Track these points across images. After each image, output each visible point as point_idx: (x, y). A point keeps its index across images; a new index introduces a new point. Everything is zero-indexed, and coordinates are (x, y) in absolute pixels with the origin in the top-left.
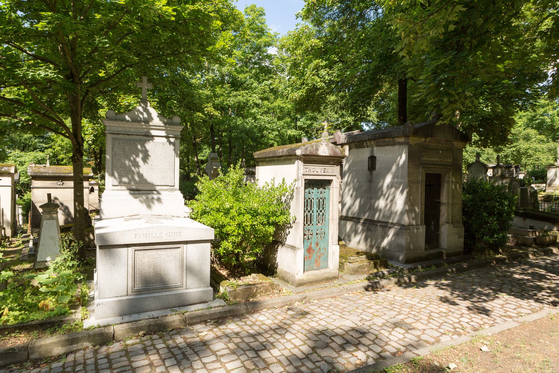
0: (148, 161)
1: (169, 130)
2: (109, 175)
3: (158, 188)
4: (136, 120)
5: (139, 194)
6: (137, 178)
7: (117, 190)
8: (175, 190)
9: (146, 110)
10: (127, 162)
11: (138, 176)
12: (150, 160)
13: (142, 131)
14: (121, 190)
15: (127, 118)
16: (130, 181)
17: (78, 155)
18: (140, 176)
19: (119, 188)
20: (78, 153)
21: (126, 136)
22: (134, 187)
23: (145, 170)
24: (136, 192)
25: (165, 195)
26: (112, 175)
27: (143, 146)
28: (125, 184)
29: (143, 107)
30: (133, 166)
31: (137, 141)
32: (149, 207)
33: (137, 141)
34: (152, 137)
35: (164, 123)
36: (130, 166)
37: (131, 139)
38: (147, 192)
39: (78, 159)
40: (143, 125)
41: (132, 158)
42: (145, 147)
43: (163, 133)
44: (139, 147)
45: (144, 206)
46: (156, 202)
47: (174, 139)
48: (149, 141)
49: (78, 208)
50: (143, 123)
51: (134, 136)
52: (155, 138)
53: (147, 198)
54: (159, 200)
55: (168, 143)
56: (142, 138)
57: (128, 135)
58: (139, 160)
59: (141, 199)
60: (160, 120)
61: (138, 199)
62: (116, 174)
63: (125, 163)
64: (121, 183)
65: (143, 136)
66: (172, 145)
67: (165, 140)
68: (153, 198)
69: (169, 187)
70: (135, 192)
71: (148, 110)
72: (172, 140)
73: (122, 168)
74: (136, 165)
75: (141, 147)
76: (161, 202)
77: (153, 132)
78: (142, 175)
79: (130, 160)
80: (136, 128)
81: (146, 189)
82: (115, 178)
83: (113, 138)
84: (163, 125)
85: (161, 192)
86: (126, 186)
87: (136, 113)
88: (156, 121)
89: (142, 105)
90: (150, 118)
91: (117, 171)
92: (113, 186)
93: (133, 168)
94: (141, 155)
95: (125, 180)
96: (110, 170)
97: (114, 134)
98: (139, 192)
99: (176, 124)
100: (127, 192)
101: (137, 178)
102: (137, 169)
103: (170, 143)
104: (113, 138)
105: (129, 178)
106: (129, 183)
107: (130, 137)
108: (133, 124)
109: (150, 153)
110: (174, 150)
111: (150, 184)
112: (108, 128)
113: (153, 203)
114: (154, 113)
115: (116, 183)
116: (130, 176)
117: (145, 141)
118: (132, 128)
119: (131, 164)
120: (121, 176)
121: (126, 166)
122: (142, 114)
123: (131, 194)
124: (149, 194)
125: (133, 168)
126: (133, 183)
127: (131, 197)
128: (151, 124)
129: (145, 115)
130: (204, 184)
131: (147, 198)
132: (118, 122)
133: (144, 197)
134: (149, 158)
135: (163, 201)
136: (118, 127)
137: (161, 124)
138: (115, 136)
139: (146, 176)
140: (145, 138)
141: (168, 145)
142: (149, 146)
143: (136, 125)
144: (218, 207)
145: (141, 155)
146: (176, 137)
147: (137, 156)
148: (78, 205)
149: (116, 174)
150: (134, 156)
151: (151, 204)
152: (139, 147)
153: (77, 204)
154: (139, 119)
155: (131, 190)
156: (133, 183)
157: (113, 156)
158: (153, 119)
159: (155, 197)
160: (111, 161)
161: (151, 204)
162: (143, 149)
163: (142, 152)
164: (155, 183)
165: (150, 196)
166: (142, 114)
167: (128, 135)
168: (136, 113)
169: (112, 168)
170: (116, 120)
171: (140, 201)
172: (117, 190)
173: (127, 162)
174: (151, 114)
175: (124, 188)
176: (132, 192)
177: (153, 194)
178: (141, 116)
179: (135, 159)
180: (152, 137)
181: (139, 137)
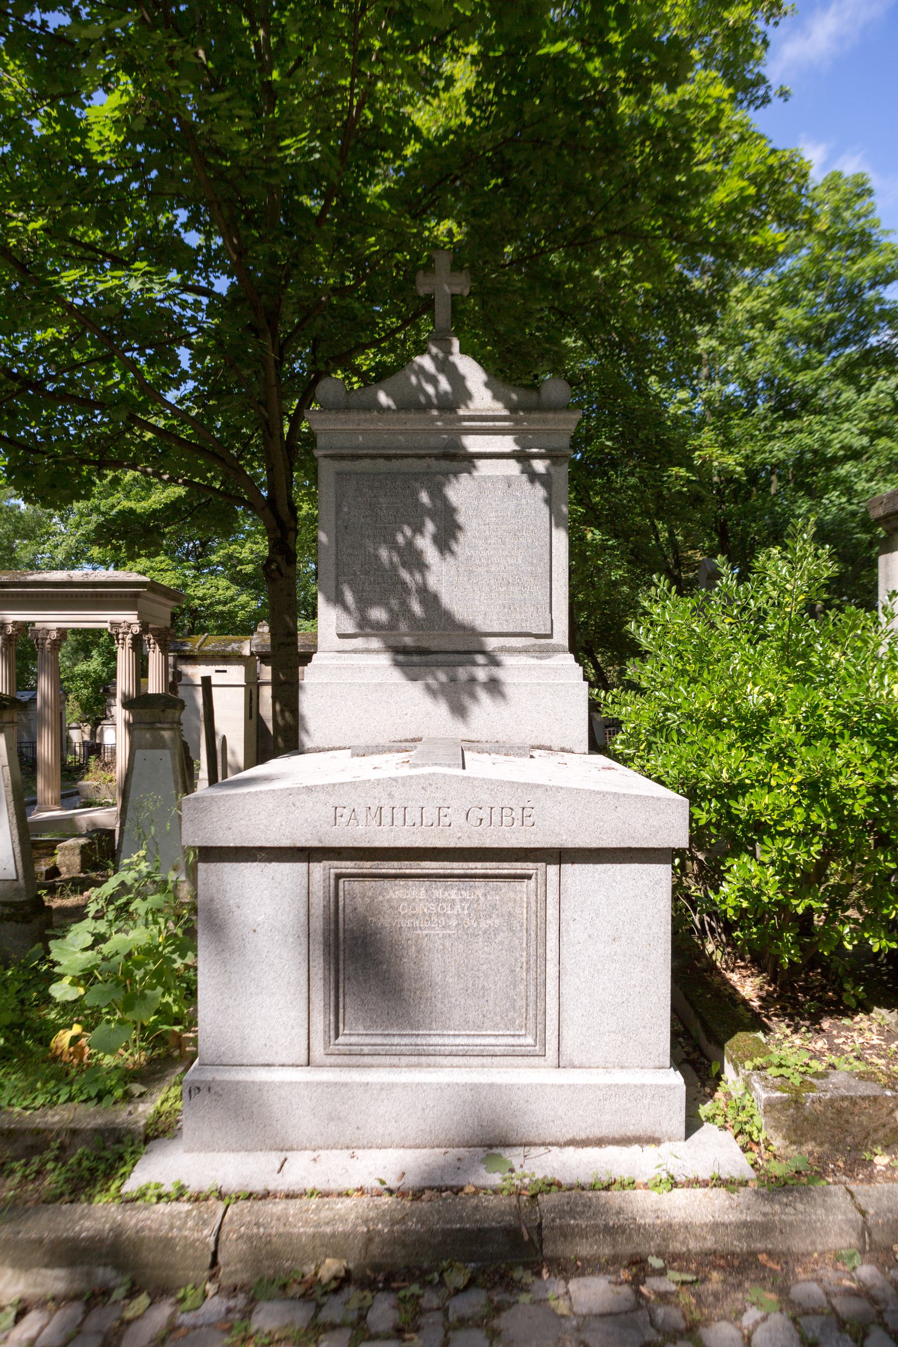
0: (455, 547)
2: (328, 600)
3: (492, 644)
4: (411, 404)
5: (427, 665)
6: (417, 608)
8: (556, 650)
10: (384, 553)
11: (422, 602)
12: (463, 546)
13: (432, 440)
14: (367, 651)
15: (383, 398)
17: (279, 558)
18: (430, 599)
19: (359, 643)
21: (381, 461)
22: (408, 641)
23: (443, 576)
24: (416, 659)
25: (516, 670)
26: (337, 600)
27: (438, 494)
29: (434, 358)
30: (404, 564)
32: (459, 711)
34: (468, 460)
35: (513, 408)
36: (394, 568)
38: (452, 658)
39: (279, 569)
41: (400, 539)
42: (445, 500)
43: (507, 444)
46: (483, 696)
47: (547, 462)
48: (456, 474)
49: (280, 721)
50: (435, 413)
52: (480, 463)
53: (453, 680)
54: (494, 686)
55: (524, 477)
57: (388, 457)
58: (425, 544)
59: (431, 681)
60: (496, 397)
61: (419, 684)
62: (349, 597)
63: (377, 557)
64: (366, 627)
65: (437, 457)
66: (538, 485)
67: (513, 468)
68: (473, 680)
69: (531, 641)
70: (412, 658)
71: (454, 366)
72: (540, 466)
73: (367, 573)
74: (416, 562)
75: (432, 496)
76: (502, 695)
77: (473, 444)
78: (435, 598)
79: (393, 546)
80: (415, 432)
81: (451, 647)
82: (346, 608)
83: (338, 473)
84: (505, 413)
85: (508, 660)
86: (384, 638)
90: (462, 393)
92: (342, 636)
93: (405, 575)
94: (430, 527)
95: (378, 614)
96: (332, 583)
99: (555, 408)
100: (384, 660)
101: (417, 608)
102: (418, 577)
103: (533, 477)
104: (338, 473)
105: (390, 611)
106: (392, 626)
107: (396, 464)
108: (403, 416)
109: (461, 519)
110: (548, 501)
112: (321, 441)
113: (473, 696)
115: (349, 627)
116: (394, 603)
118: (401, 432)
119: (396, 559)
120: (364, 604)
122: (434, 381)
123: (397, 664)
124: (461, 664)
125: (405, 575)
126: (403, 627)
127: (396, 676)
128: (461, 412)
129: (444, 385)
130: (663, 616)
131: (453, 680)
132: (354, 416)
133: (442, 677)
134: (461, 537)
135: (508, 690)
137: (499, 409)
138: (346, 465)
139: (448, 600)
140: (444, 464)
141: (527, 486)
142: (460, 492)
143: (413, 422)
144: (714, 706)
145: (430, 527)
146: (551, 456)
147: (419, 529)
148: (282, 711)
149: (349, 597)
150: (408, 532)
151: (467, 701)
152: (424, 497)
153: (278, 707)
154: (423, 399)
156: (403, 627)
157: (341, 532)
159: (481, 674)
160: (333, 551)
161: (467, 701)
162: (439, 504)
164: (482, 625)
165: (462, 673)
166: (434, 381)
167: (388, 457)
168: (414, 380)
169: (337, 576)
171: (429, 689)
172: (355, 651)
174: (462, 378)
175: (375, 643)
176: (401, 658)
177: (475, 664)
178: (430, 389)
179: (410, 543)
180: (468, 460)
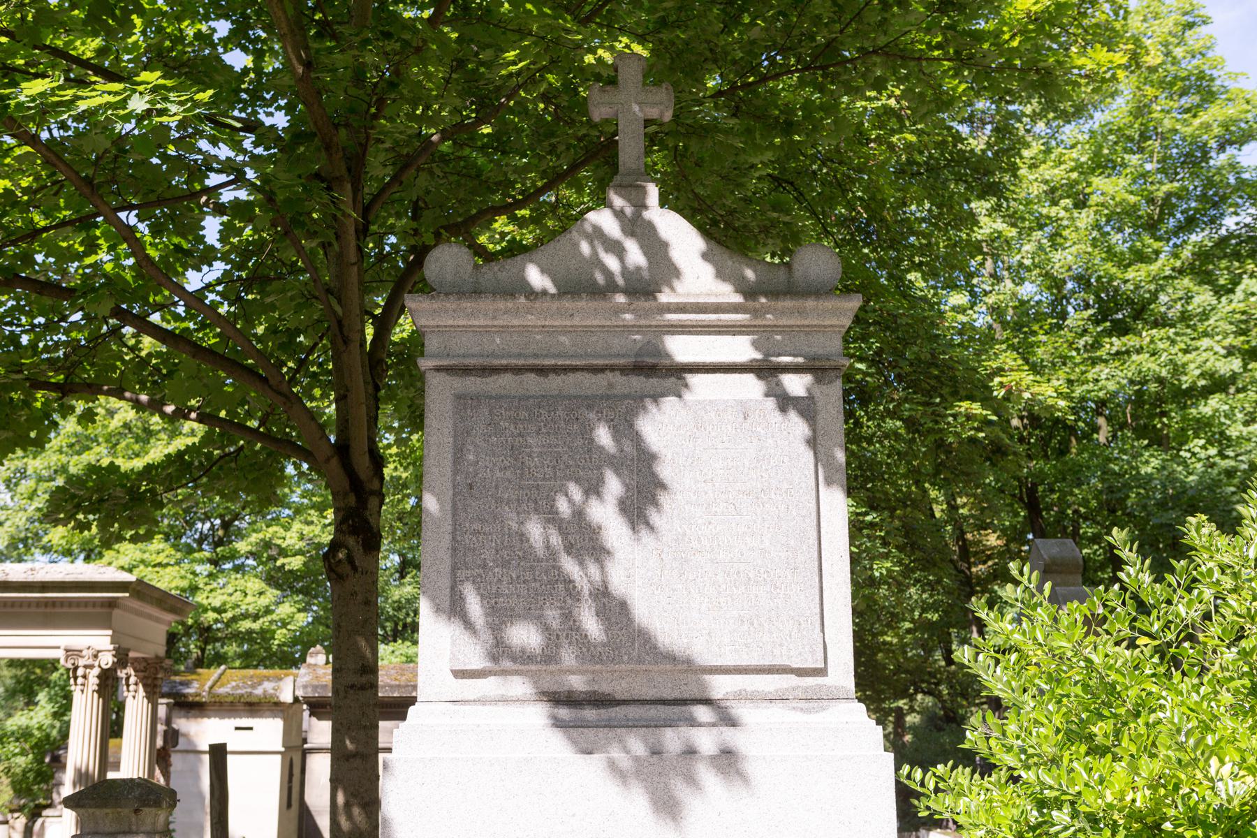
0: (654, 518)
1: (774, 328)
2: (438, 610)
3: (720, 686)
4: (580, 285)
5: (609, 725)
6: (592, 625)
7: (482, 701)
8: (833, 697)
9: (637, 227)
10: (535, 530)
11: (602, 613)
12: (670, 514)
13: (617, 343)
14: (505, 700)
15: (535, 277)
16: (553, 640)
17: (351, 541)
18: (614, 610)
19: (490, 686)
20: (354, 531)
21: (531, 378)
22: (577, 683)
23: (640, 570)
24: (590, 714)
25: (764, 731)
26: (455, 609)
27: (625, 429)
28: (518, 661)
29: (619, 214)
30: (569, 549)
31: (590, 401)
32: (667, 807)
33: (590, 401)
34: (676, 375)
35: (749, 292)
36: (552, 554)
37: (560, 397)
38: (653, 711)
39: (350, 559)
40: (619, 310)
41: (563, 506)
42: (637, 439)
43: (741, 349)
44: (603, 436)
45: (637, 802)
46: (708, 777)
47: (807, 379)
48: (656, 398)
49: (344, 824)
50: (621, 299)
51: (572, 378)
52: (693, 379)
53: (656, 752)
54: (727, 759)
55: (771, 403)
56: (622, 383)
57: (541, 371)
58: (605, 513)
59: (616, 754)
60: (721, 275)
61: (597, 760)
62: (474, 606)
63: (523, 537)
64: (503, 656)
65: (624, 370)
66: (793, 415)
67: (751, 386)
68: (690, 752)
69: (792, 680)
70: (583, 711)
71: (651, 226)
72: (796, 384)
73: (505, 564)
74: (589, 544)
75: (617, 434)
76: (743, 777)
77: (682, 349)
78: (623, 606)
79: (551, 517)
80: (588, 330)
81: (651, 694)
82: (468, 625)
83: (459, 397)
84: (738, 299)
86: (534, 677)
87: (585, 248)
88: (696, 271)
89: (618, 202)
90: (663, 268)
91: (478, 583)
92: (460, 674)
93: (570, 566)
94: (613, 486)
95: (525, 635)
96: (445, 583)
97: (466, 371)
98: (604, 713)
99: (816, 291)
100: (538, 714)
101: (592, 625)
102: (593, 569)
103: (785, 402)
104: (459, 397)
105: (546, 629)
106: (549, 656)
107: (554, 383)
108: (567, 304)
109: (665, 471)
110: (812, 443)
111: (672, 658)
112: (432, 343)
113: (691, 780)
114: (682, 237)
115: (475, 658)
116: (552, 616)
117: (637, 403)
118: (565, 331)
119: (556, 540)
120: (500, 616)
121: (527, 553)
122: (617, 249)
123: (558, 723)
124: (670, 723)
125: (570, 566)
126: (568, 657)
127: (557, 745)
128: (665, 297)
129: (635, 255)
130: (1026, 638)
131: (656, 752)
132: (486, 304)
133: (637, 745)
134: (663, 498)
135: (752, 768)
136: (486, 331)
137: (726, 293)
138: (472, 384)
139: (644, 612)
140: (637, 383)
141: (776, 416)
142: (661, 426)
143: (585, 313)
144: (1142, 799)
145: (613, 486)
146: (816, 368)
147: (594, 489)
148: (347, 805)
149: (474, 606)
150: (576, 493)
151: (680, 789)
152: (603, 436)
153: (341, 799)
154: (600, 278)
155: (558, 699)
156: (568, 657)
157: (465, 492)
158: (676, 272)
159: (706, 741)
160: (447, 527)
161: (680, 789)
162: (628, 446)
163: (617, 464)
164: (705, 654)
165: (672, 739)
166: (617, 249)
167: (541, 371)
168: (585, 248)
169: (454, 569)
170: (477, 292)
171: (613, 766)
172: (482, 701)
173: (535, 530)
174: (665, 245)
175: (519, 686)
176: (564, 713)
177: (693, 722)
178: (612, 263)
179: (579, 514)
180: (676, 375)
181: (601, 381)
